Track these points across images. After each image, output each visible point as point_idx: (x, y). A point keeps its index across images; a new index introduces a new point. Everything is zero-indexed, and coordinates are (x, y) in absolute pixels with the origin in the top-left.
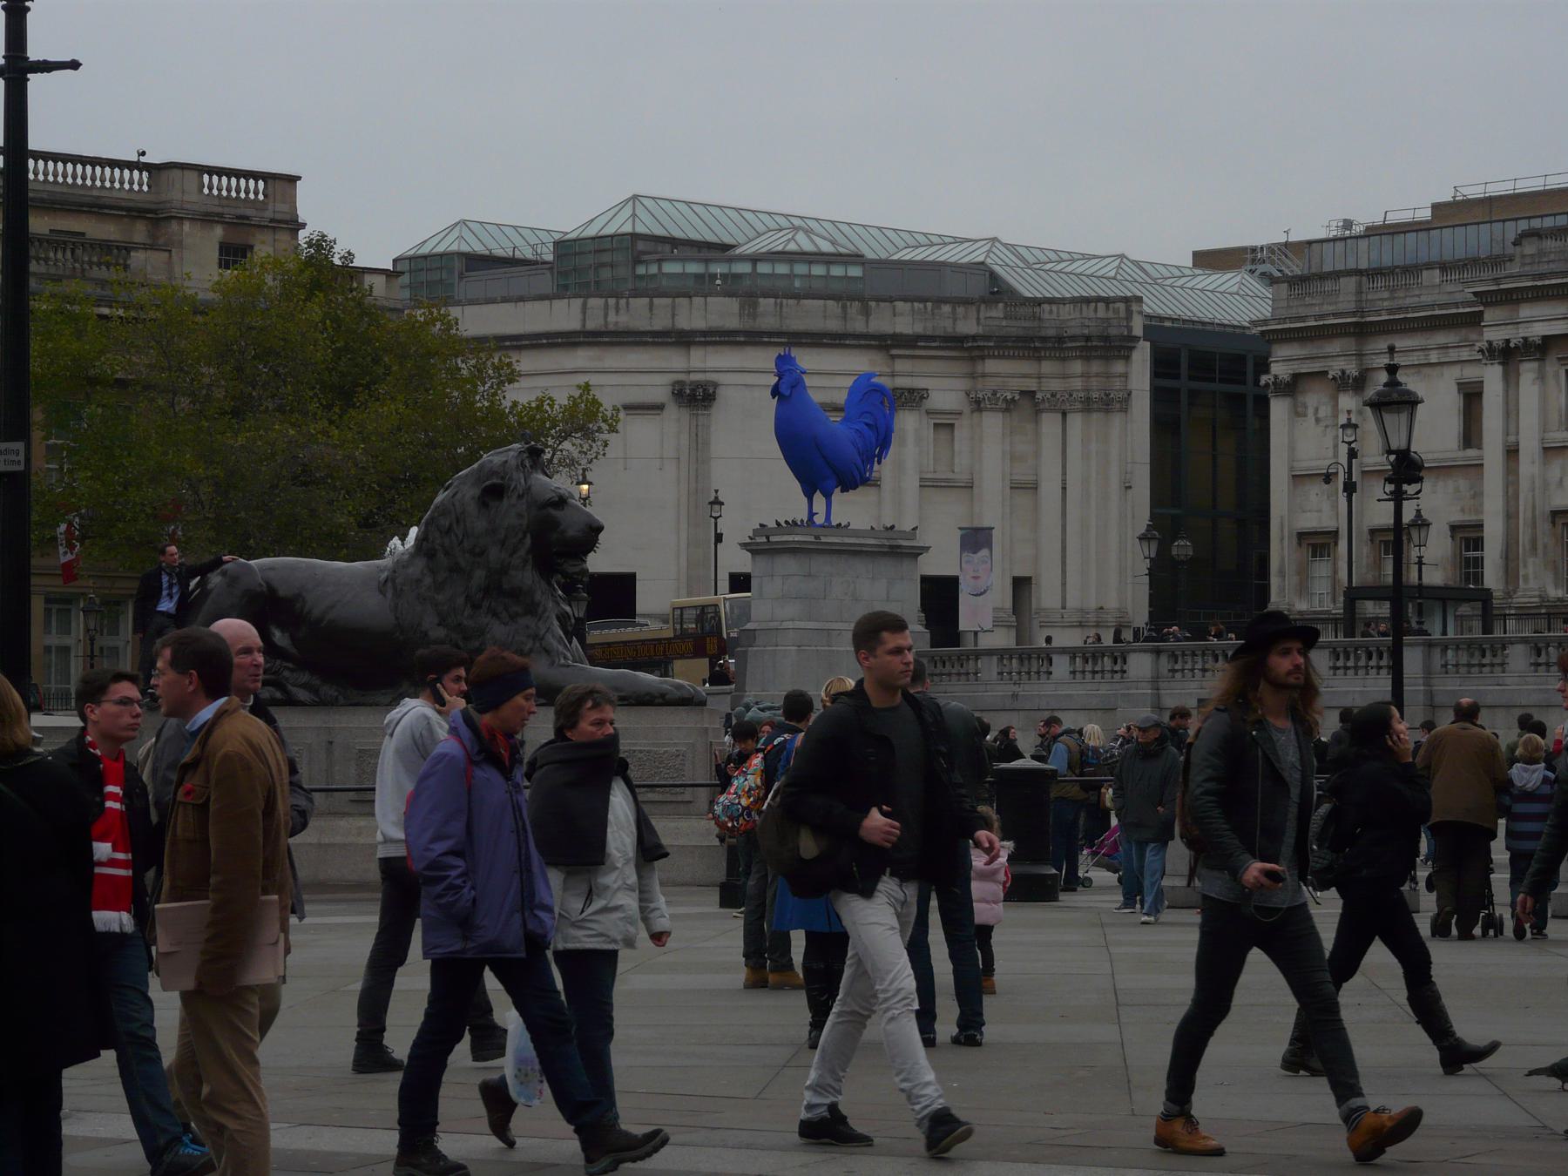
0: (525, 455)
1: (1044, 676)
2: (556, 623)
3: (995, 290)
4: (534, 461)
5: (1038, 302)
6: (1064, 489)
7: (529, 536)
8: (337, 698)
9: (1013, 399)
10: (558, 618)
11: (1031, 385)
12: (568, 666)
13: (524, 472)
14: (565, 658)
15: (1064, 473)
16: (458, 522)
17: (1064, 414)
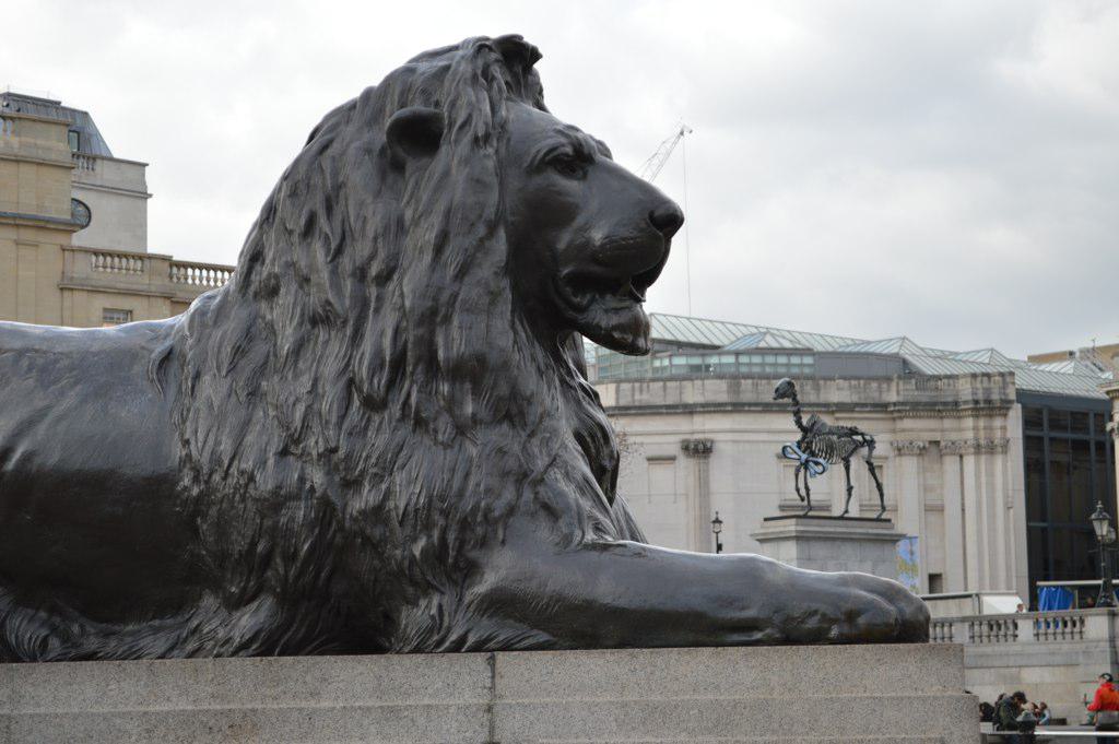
0: (494, 56)
1: (1010, 639)
2: (572, 444)
3: (906, 370)
4: (515, 75)
5: (938, 378)
6: (963, 510)
7: (502, 233)
8: (45, 640)
9: (924, 447)
10: (579, 437)
11: (937, 436)
12: (606, 547)
13: (489, 90)
14: (598, 528)
15: (963, 499)
16: (329, 209)
17: (961, 457)
